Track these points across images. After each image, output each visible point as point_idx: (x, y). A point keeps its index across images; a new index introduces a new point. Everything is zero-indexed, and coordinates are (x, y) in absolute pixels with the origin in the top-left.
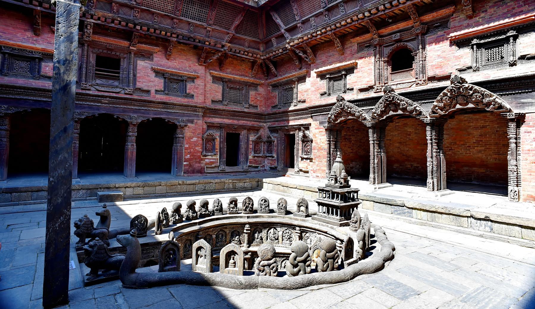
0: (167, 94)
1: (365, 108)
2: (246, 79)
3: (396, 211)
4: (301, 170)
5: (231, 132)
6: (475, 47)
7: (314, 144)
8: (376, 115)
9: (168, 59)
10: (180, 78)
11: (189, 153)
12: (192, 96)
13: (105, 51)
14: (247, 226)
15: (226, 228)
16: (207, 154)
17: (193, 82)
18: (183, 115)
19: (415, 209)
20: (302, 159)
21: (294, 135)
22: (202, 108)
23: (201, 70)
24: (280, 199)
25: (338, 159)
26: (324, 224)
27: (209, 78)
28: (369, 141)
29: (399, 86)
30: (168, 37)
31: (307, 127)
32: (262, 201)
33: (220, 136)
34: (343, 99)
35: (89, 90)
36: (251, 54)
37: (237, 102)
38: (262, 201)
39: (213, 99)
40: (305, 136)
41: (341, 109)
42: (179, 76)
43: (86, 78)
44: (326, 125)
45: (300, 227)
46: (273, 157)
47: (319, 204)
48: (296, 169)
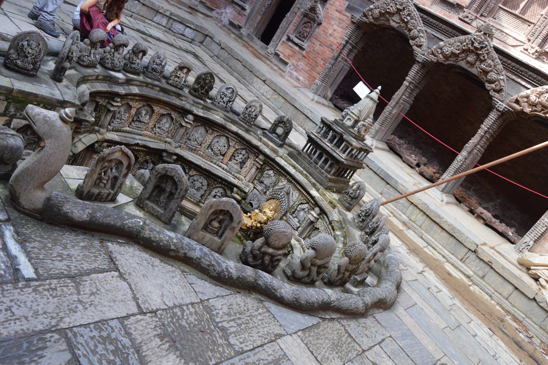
1: (429, 31)
4: (277, 55)
26: (305, 172)
28: (404, 80)
32: (228, 89)
38: (228, 89)
41: (398, 9)
44: (358, 16)
46: (243, 9)
47: (310, 140)
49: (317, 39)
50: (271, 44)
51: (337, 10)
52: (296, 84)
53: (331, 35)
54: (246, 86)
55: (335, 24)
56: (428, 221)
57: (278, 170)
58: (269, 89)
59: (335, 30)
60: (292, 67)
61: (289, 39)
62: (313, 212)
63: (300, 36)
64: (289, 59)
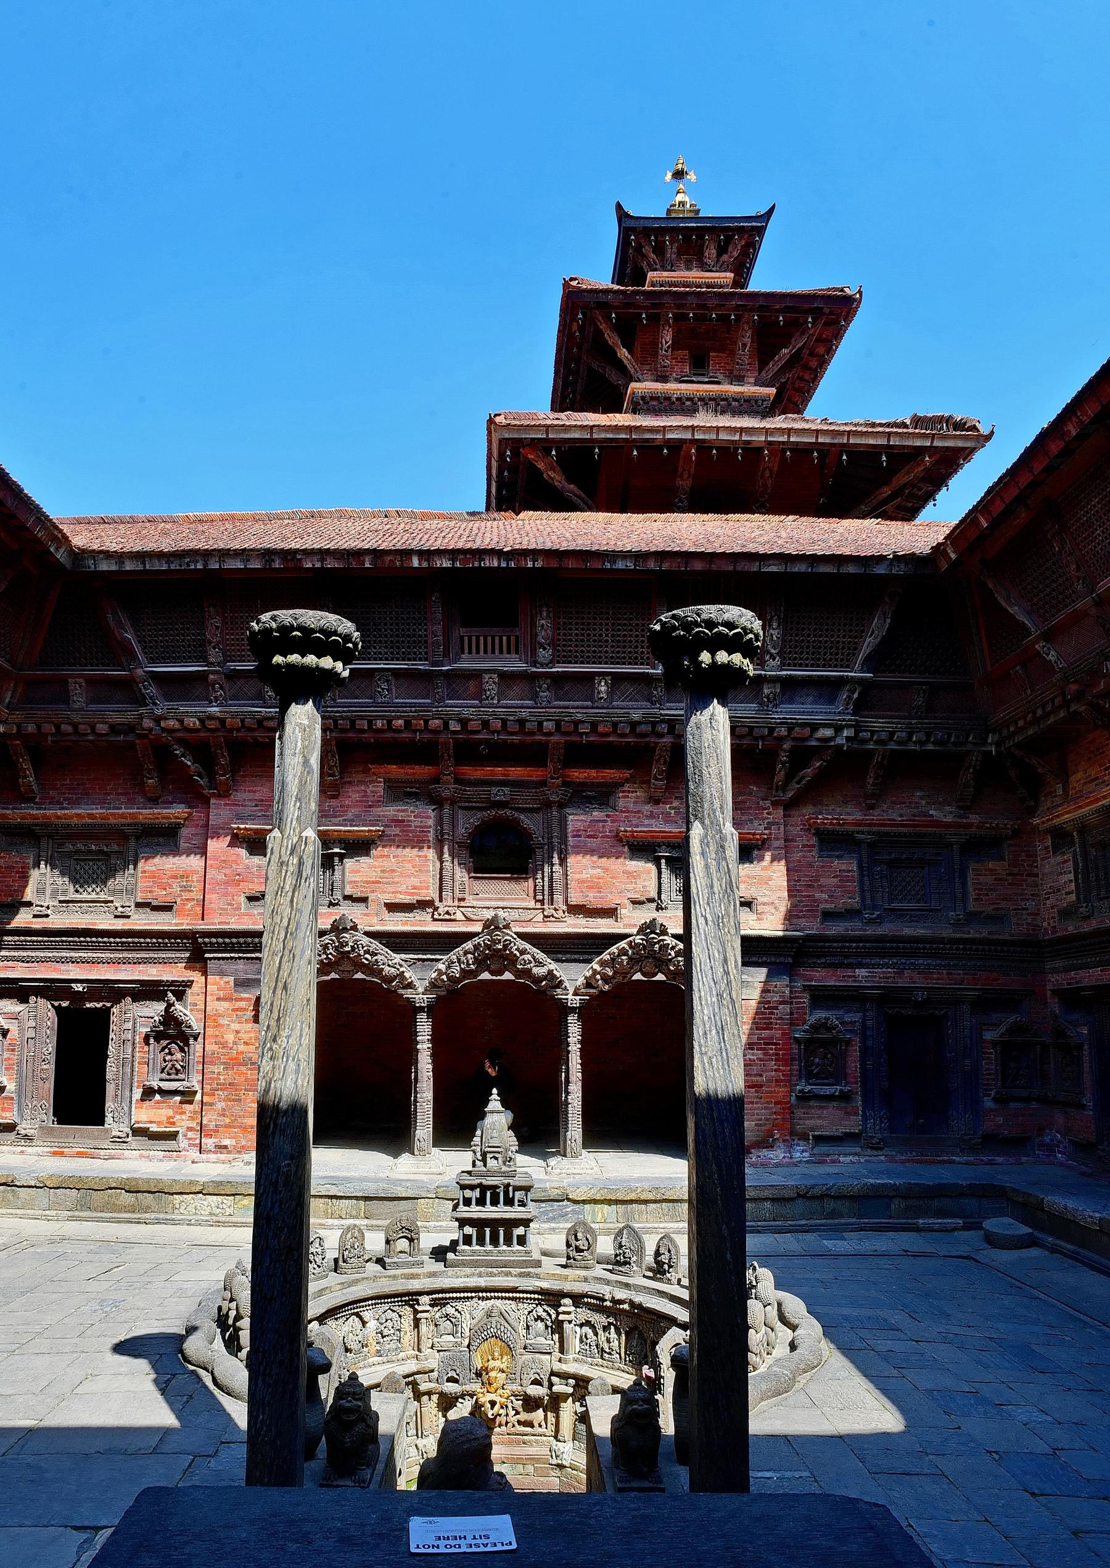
3: (545, 1213)
4: (138, 1132)
6: (663, 861)
7: (196, 1047)
8: (444, 977)
19: (595, 1202)
20: (148, 1093)
21: (106, 1012)
24: (349, 1229)
25: (495, 1103)
29: (515, 915)
31: (180, 990)
34: (354, 928)
40: (169, 1018)
45: (428, 1293)
48: (114, 1125)
49: (212, 1063)
50: (109, 1119)
51: (218, 999)
52: (223, 1157)
53: (235, 1043)
54: (165, 1222)
55: (232, 1021)
56: (621, 1208)
57: (457, 1298)
58: (220, 1198)
59: (237, 1032)
60: (190, 1134)
61: (148, 1093)
62: (561, 1309)
63: (169, 1074)
64: (173, 1123)
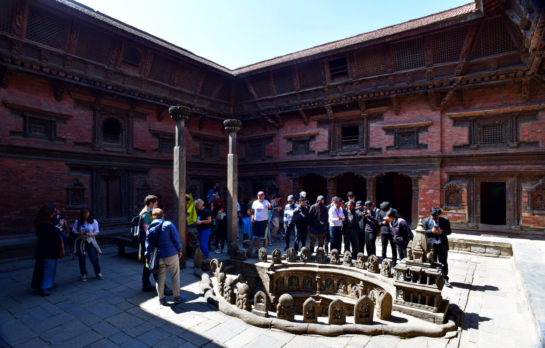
0: (399, 149)
2: (508, 109)
5: (488, 181)
9: (397, 115)
10: (410, 130)
11: (425, 206)
12: (426, 146)
13: (346, 123)
14: (361, 282)
15: (347, 278)
16: (449, 207)
17: (427, 131)
18: (416, 167)
22: (437, 157)
23: (436, 116)
27: (448, 122)
30: (388, 95)
33: (468, 188)
35: (336, 156)
36: (503, 76)
37: (496, 140)
39: (456, 145)
42: (409, 128)
43: (334, 147)
